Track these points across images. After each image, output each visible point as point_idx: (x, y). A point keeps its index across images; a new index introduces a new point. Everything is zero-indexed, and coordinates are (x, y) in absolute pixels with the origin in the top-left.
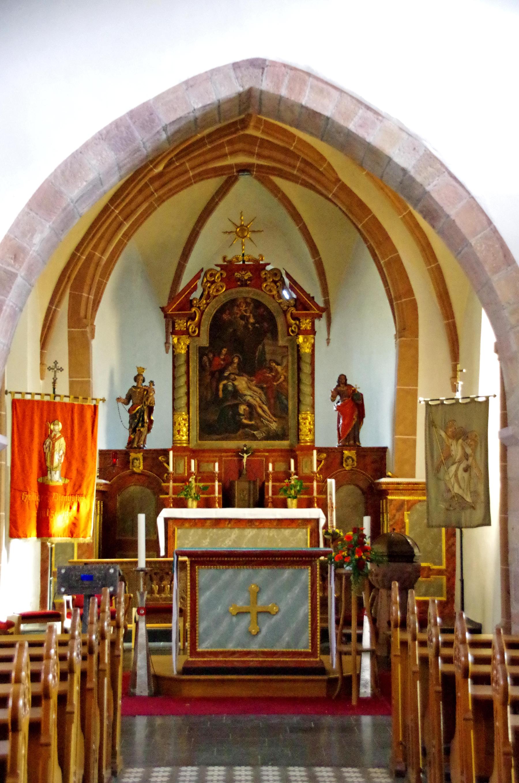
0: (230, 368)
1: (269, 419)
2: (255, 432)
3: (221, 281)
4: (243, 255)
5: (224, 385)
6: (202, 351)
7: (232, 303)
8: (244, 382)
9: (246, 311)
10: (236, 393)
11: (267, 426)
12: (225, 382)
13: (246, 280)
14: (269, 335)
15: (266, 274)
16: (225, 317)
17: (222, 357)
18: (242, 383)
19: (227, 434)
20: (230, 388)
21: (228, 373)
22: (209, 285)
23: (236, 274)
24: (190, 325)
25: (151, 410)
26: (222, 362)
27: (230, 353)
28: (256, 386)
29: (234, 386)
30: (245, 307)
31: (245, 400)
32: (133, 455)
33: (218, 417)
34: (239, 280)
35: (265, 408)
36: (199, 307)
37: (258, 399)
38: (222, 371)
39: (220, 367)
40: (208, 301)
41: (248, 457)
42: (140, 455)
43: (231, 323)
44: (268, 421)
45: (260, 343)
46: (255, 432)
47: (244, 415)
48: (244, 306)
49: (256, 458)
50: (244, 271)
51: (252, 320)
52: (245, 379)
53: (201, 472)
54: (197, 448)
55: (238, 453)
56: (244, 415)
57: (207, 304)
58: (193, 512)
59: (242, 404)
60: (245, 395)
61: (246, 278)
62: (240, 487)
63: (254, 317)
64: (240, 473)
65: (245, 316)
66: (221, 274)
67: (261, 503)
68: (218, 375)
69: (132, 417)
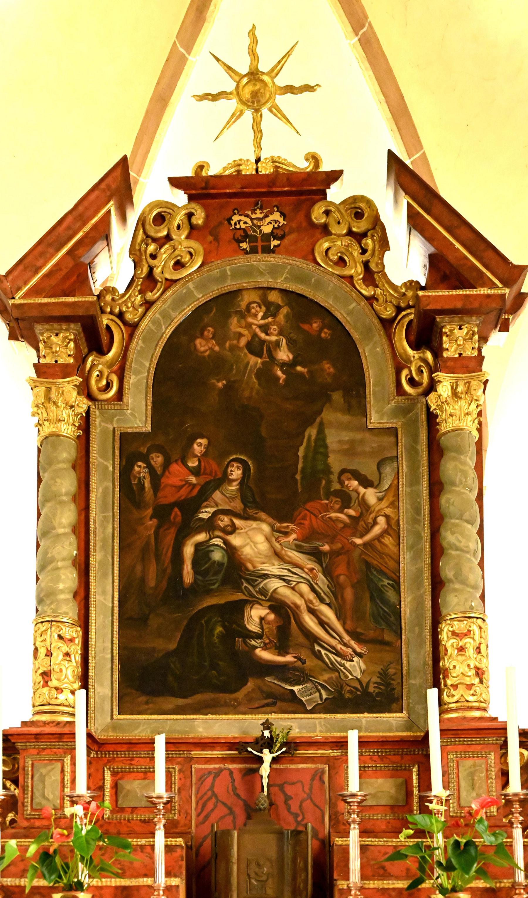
0: (217, 495)
1: (339, 646)
2: (295, 688)
3: (188, 237)
4: (258, 161)
5: (198, 546)
6: (130, 448)
7: (225, 303)
8: (260, 538)
9: (265, 328)
10: (235, 570)
11: (334, 669)
12: (201, 537)
13: (267, 237)
14: (337, 397)
15: (327, 213)
16: (202, 346)
17: (193, 463)
18: (253, 540)
19: (208, 696)
20: (217, 556)
21: (211, 510)
22: (152, 248)
23: (236, 218)
24: (93, 366)
26: (193, 479)
28: (299, 549)
29: (231, 550)
30: (263, 318)
31: (263, 592)
34: (245, 236)
35: (329, 613)
36: (121, 316)
37: (304, 588)
38: (191, 506)
39: (183, 493)
40: (150, 296)
41: (275, 760)
43: (218, 364)
44: (338, 654)
45: (309, 422)
46: (295, 688)
47: (259, 636)
48: (261, 315)
49: (301, 766)
50: (261, 208)
51: (284, 355)
52: (266, 528)
53: (122, 810)
54: (112, 735)
56: (259, 636)
57: (148, 305)
59: (252, 602)
60: (266, 576)
61: (267, 229)
63: (291, 345)
64: (251, 811)
65: (263, 342)
66: (190, 215)
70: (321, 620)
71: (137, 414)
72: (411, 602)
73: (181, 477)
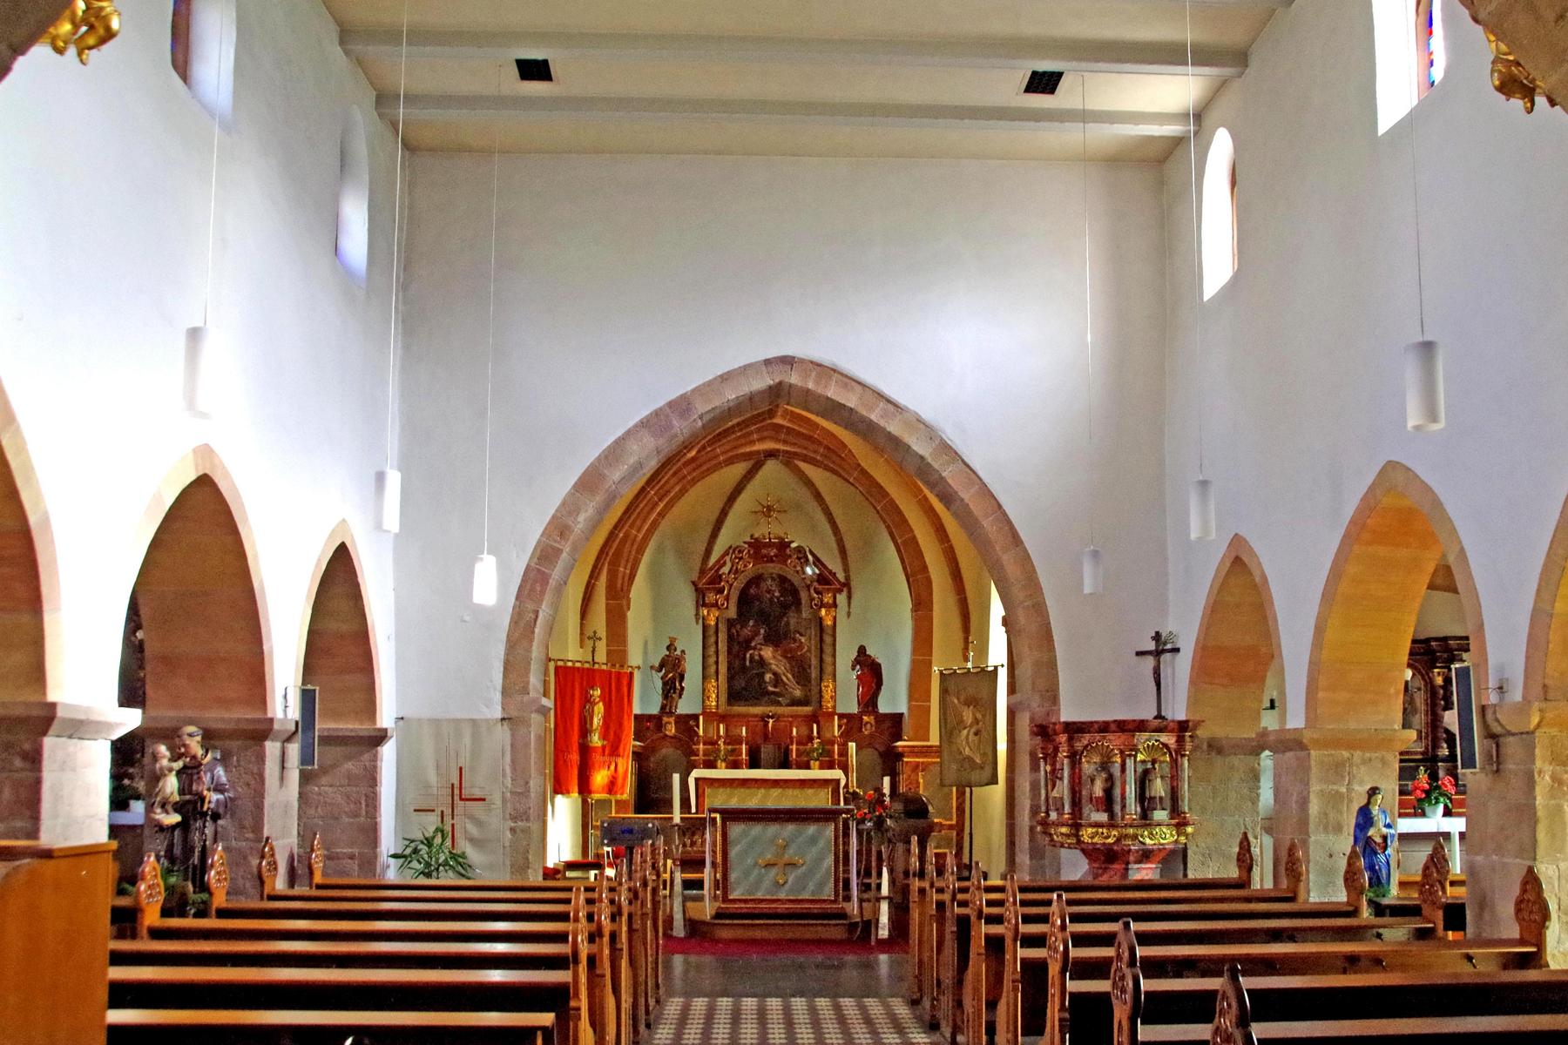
6: (731, 623)
7: (756, 580)
10: (762, 662)
18: (767, 653)
25: (682, 678)
27: (756, 625)
32: (665, 719)
33: (745, 684)
38: (748, 641)
42: (672, 720)
55: (764, 718)
58: (722, 773)
62: (767, 751)
67: (785, 764)
68: (747, 644)
69: (665, 684)
70: (788, 678)
71: (732, 613)
72: (814, 674)
73: (746, 632)
